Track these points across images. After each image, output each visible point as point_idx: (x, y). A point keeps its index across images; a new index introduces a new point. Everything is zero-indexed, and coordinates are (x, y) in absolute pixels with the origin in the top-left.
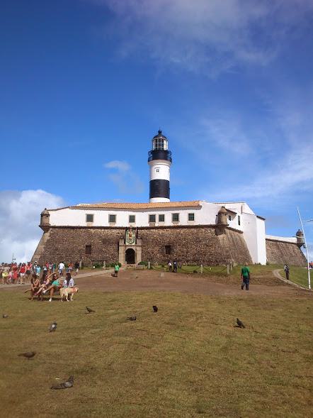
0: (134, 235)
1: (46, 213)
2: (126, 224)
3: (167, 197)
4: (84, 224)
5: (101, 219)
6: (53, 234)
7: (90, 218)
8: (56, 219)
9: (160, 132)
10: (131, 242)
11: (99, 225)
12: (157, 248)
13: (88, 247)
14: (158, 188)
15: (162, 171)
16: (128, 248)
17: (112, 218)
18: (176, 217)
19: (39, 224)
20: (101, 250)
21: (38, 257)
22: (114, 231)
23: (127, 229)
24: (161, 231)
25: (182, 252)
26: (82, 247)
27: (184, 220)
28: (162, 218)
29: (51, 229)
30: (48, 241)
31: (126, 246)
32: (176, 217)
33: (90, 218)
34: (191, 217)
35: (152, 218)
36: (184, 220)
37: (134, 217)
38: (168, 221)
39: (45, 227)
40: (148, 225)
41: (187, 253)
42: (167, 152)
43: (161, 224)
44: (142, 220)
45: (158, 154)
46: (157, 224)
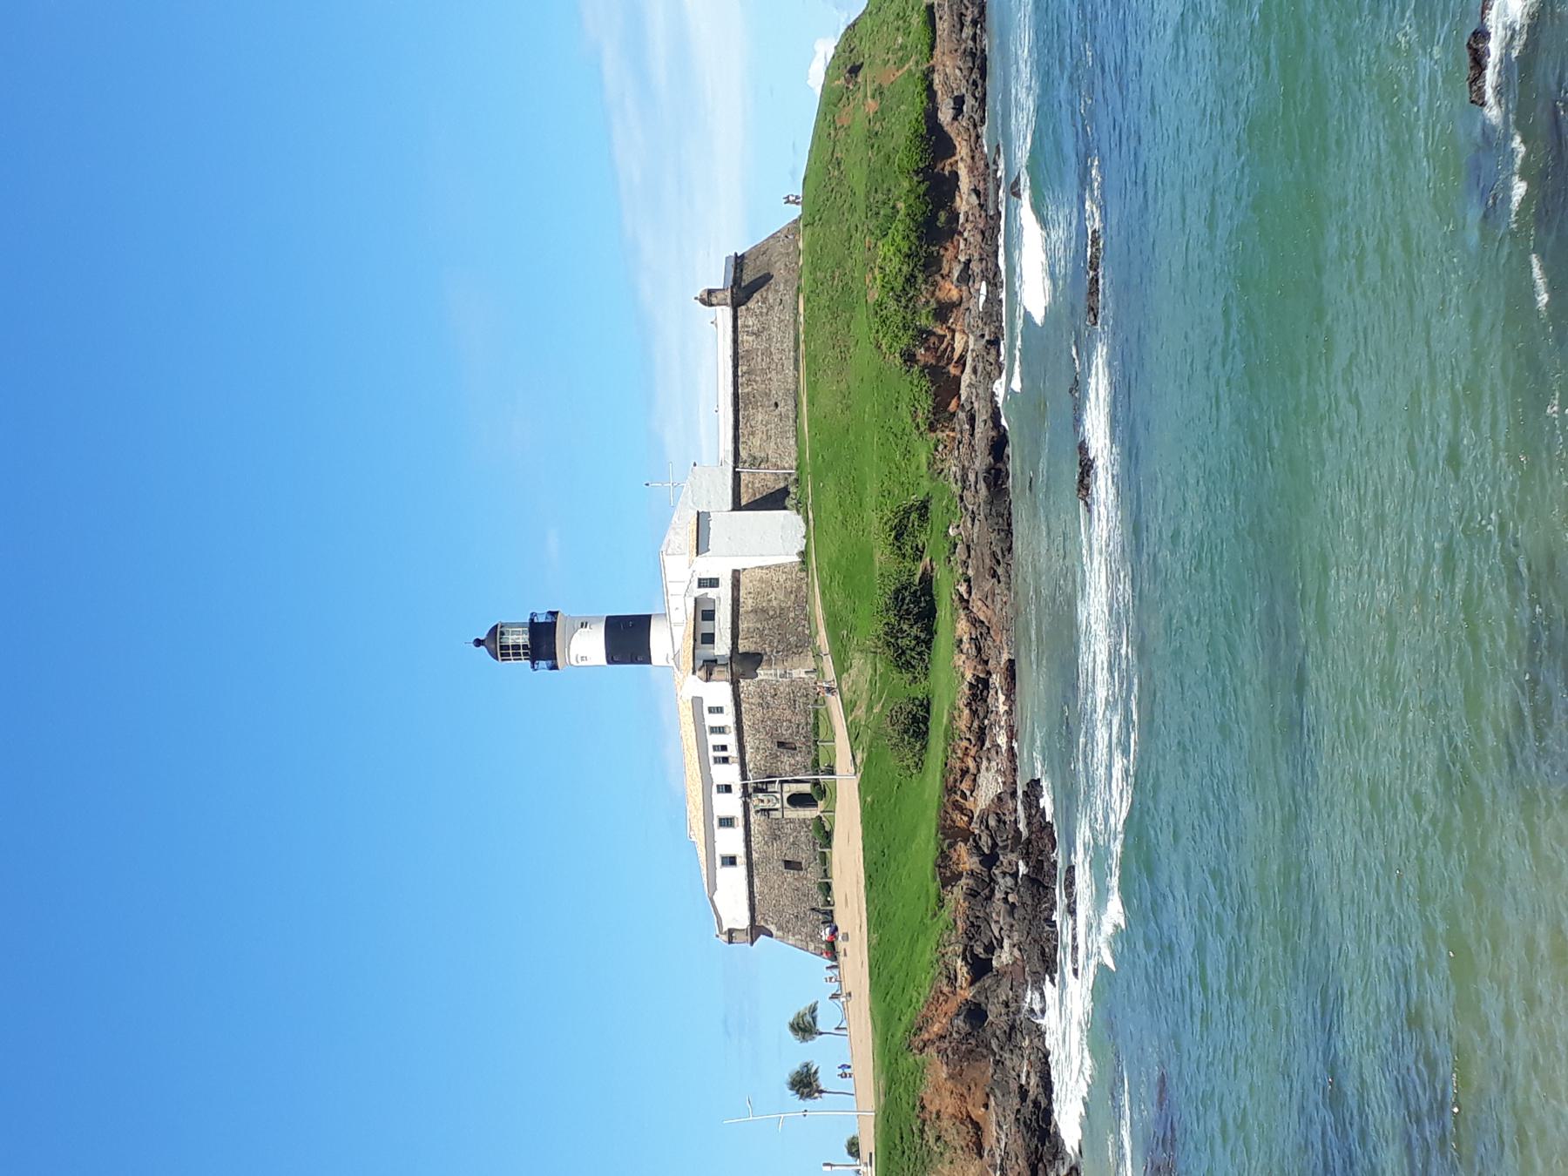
0: (760, 796)
2: (736, 795)
4: (741, 870)
8: (737, 916)
13: (788, 864)
22: (753, 817)
26: (790, 875)
33: (731, 861)
36: (727, 719)
39: (756, 930)
46: (733, 752)
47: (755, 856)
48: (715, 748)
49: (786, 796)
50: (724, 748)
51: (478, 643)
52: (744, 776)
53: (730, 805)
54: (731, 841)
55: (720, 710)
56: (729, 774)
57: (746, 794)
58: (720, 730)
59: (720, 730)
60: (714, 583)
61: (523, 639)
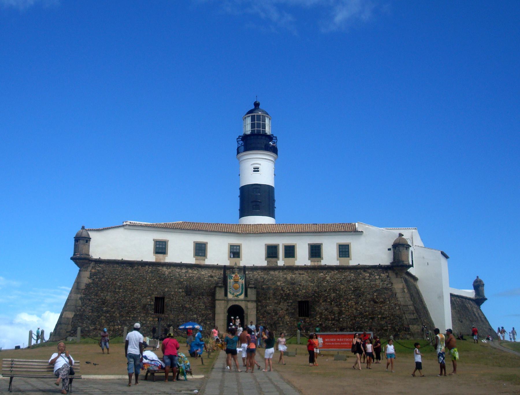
0: (242, 281)
1: (84, 234)
3: (271, 214)
4: (151, 257)
5: (181, 250)
6: (95, 274)
7: (161, 248)
9: (257, 105)
10: (235, 295)
11: (178, 261)
12: (284, 306)
14: (256, 200)
15: (260, 170)
16: (230, 304)
17: (200, 250)
18: (315, 251)
19: (72, 255)
20: (184, 307)
22: (203, 272)
23: (225, 268)
24: (289, 276)
25: (332, 312)
26: (149, 301)
27: (330, 257)
28: (290, 251)
29: (92, 264)
30: (88, 286)
31: (228, 301)
32: (315, 251)
33: (161, 248)
34: (344, 251)
35: (272, 252)
36: (330, 257)
37: (239, 246)
38: (302, 258)
40: (264, 263)
41: (340, 313)
42: (270, 138)
43: (290, 262)
44: (254, 255)
45: (256, 141)
49: (243, 305)
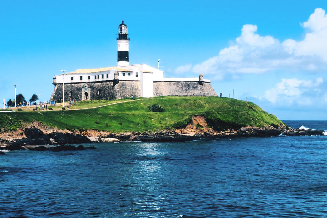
2: (87, 80)
4: (70, 81)
6: (58, 87)
11: (76, 82)
14: (123, 56)
15: (123, 46)
16: (85, 92)
21: (52, 97)
22: (82, 84)
29: (57, 85)
33: (72, 79)
36: (105, 79)
39: (55, 84)
45: (123, 37)
46: (97, 80)
47: (73, 85)
48: (98, 76)
49: (87, 92)
50: (98, 78)
51: (123, 22)
52: (92, 82)
53: (85, 79)
54: (77, 79)
55: (107, 77)
56: (92, 79)
57: (88, 82)
58: (103, 77)
59: (103, 77)
60: (137, 76)
61: (124, 32)
